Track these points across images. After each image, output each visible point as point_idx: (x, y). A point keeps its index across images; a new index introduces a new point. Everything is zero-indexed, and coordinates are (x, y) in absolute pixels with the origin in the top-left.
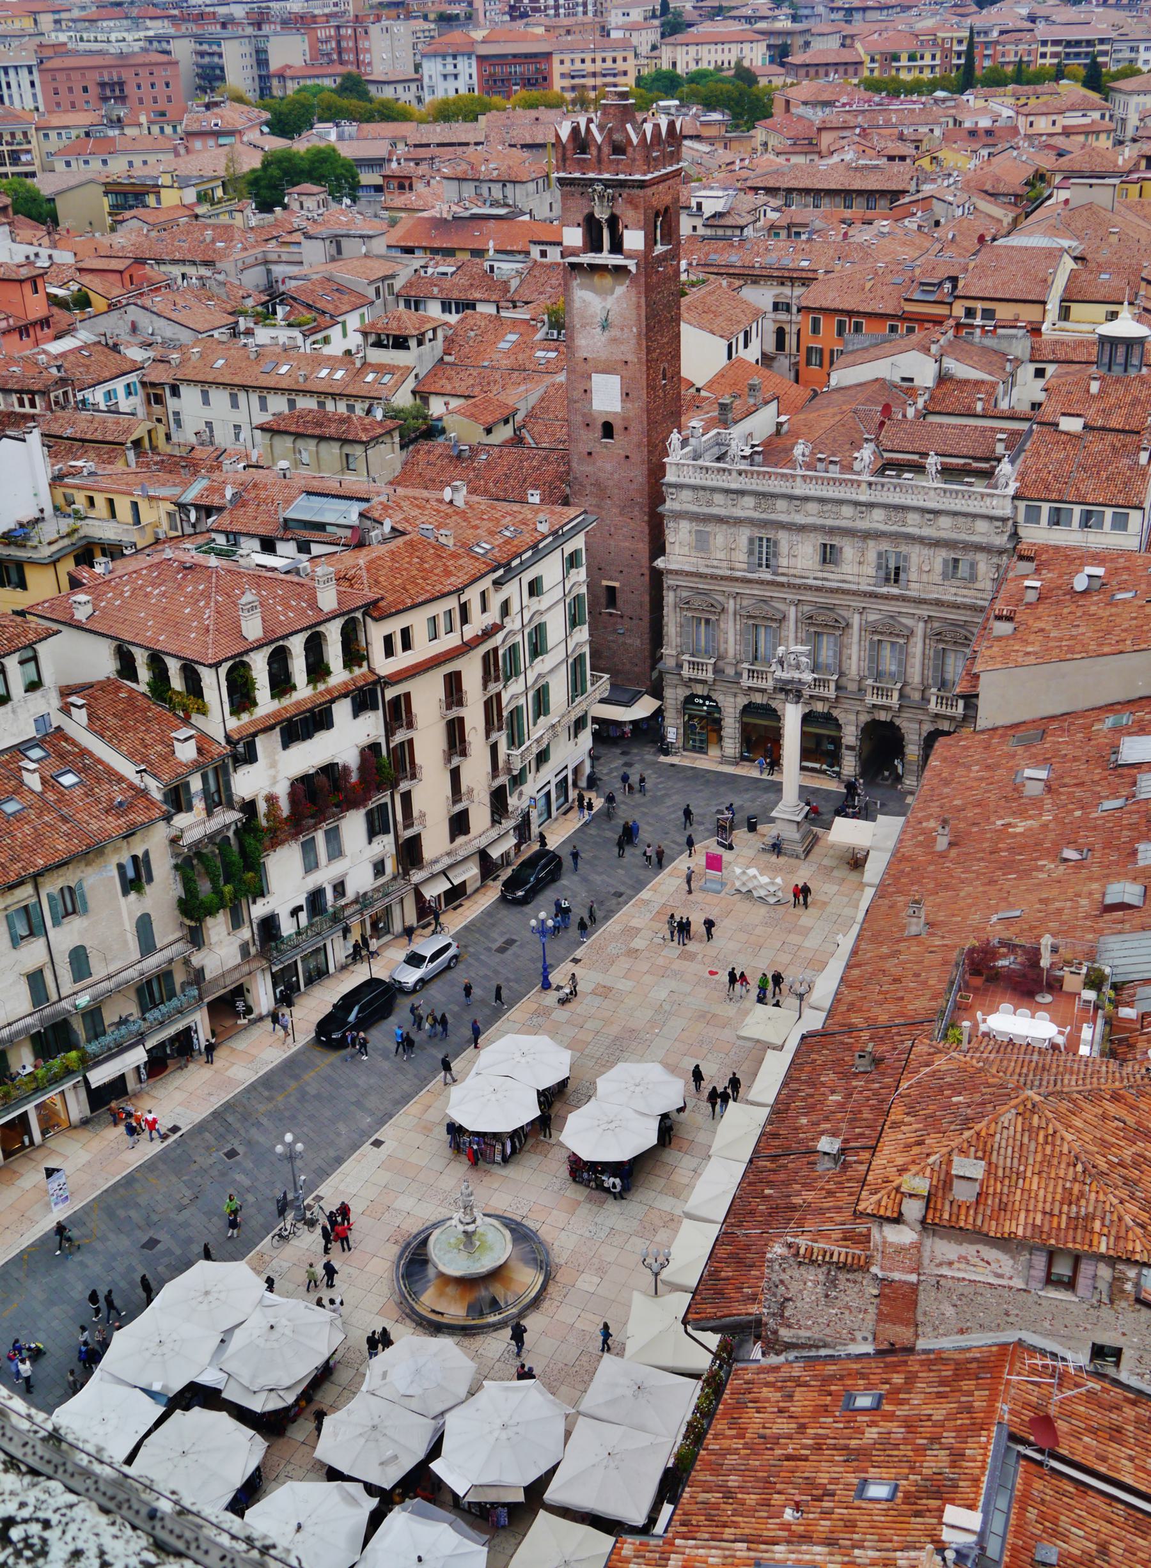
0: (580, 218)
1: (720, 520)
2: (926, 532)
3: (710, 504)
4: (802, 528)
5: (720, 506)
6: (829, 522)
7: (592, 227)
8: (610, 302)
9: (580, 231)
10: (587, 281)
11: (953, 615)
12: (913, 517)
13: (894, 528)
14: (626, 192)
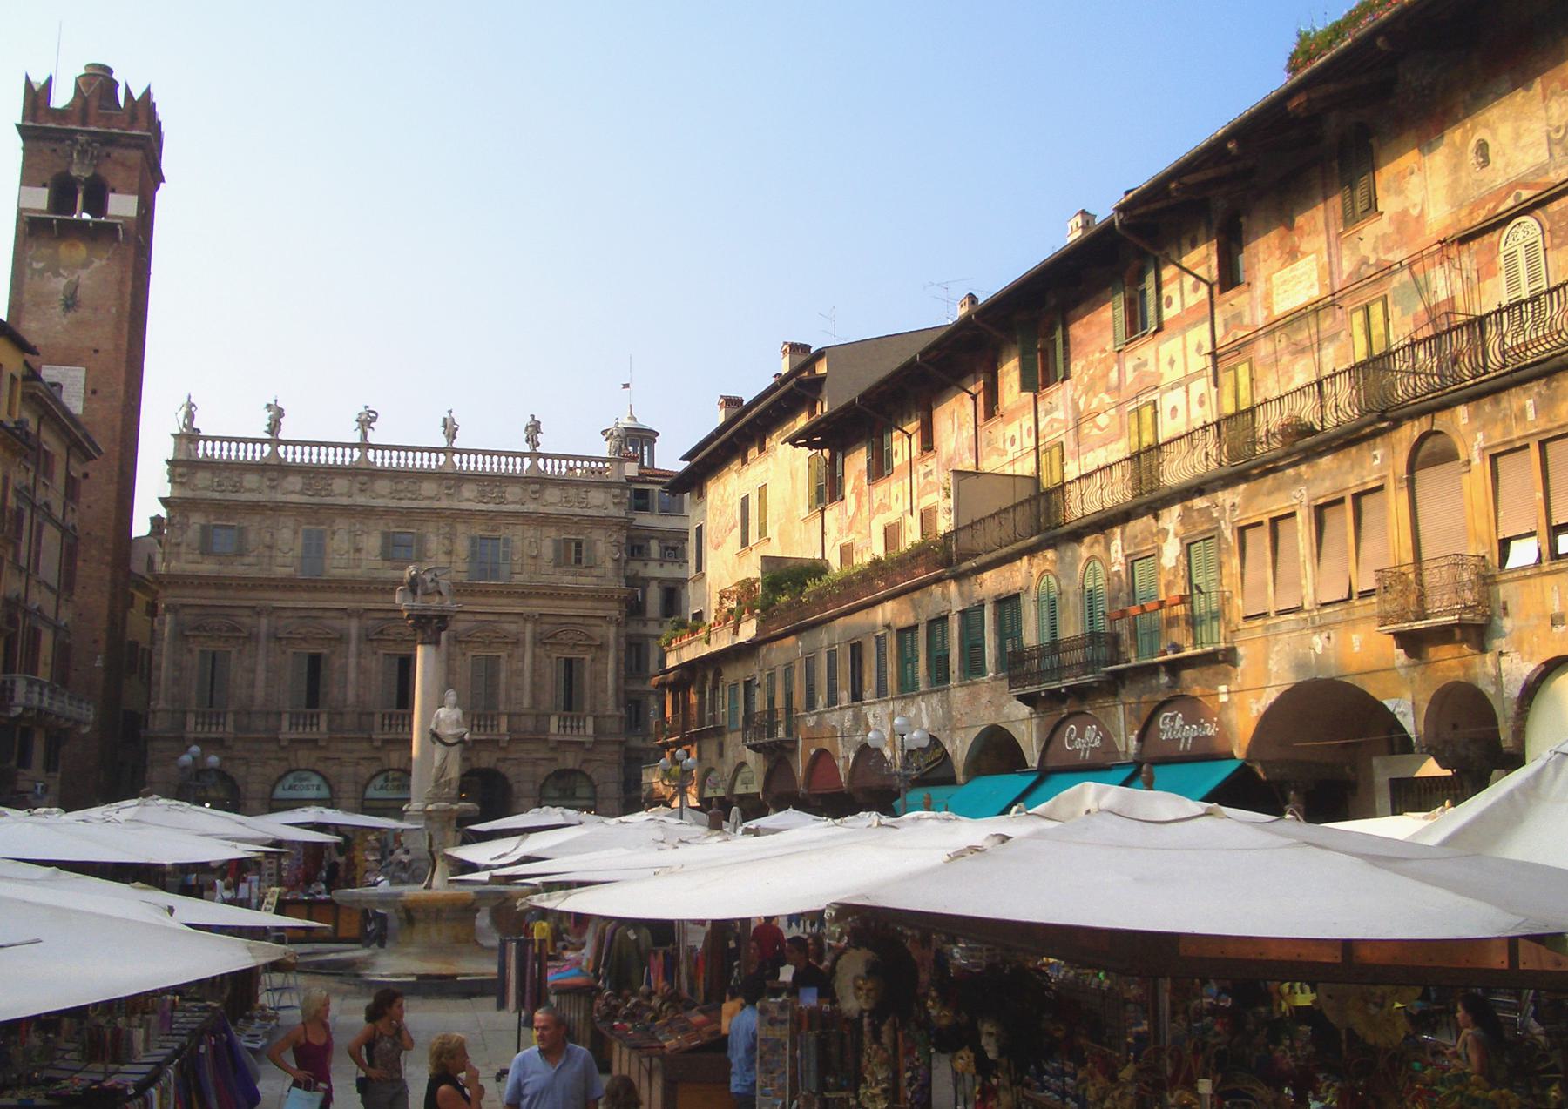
0: (47, 178)
1: (254, 507)
3: (237, 488)
4: (368, 512)
5: (253, 489)
6: (405, 504)
8: (84, 274)
9: (46, 191)
10: (47, 251)
11: (569, 608)
12: (513, 492)
13: (491, 507)
14: (117, 153)
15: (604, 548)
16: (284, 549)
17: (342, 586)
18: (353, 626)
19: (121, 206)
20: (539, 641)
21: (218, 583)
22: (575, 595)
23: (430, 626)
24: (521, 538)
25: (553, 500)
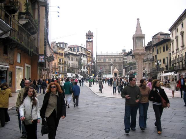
1: (101, 58)
2: (117, 57)
4: (108, 58)
5: (101, 57)
7: (88, 39)
11: (120, 63)
12: (116, 56)
15: (122, 59)
16: (102, 60)
17: (107, 62)
18: (107, 65)
19: (92, 40)
20: (118, 65)
21: (99, 62)
22: (120, 62)
23: (111, 65)
24: (117, 59)
25: (118, 57)
